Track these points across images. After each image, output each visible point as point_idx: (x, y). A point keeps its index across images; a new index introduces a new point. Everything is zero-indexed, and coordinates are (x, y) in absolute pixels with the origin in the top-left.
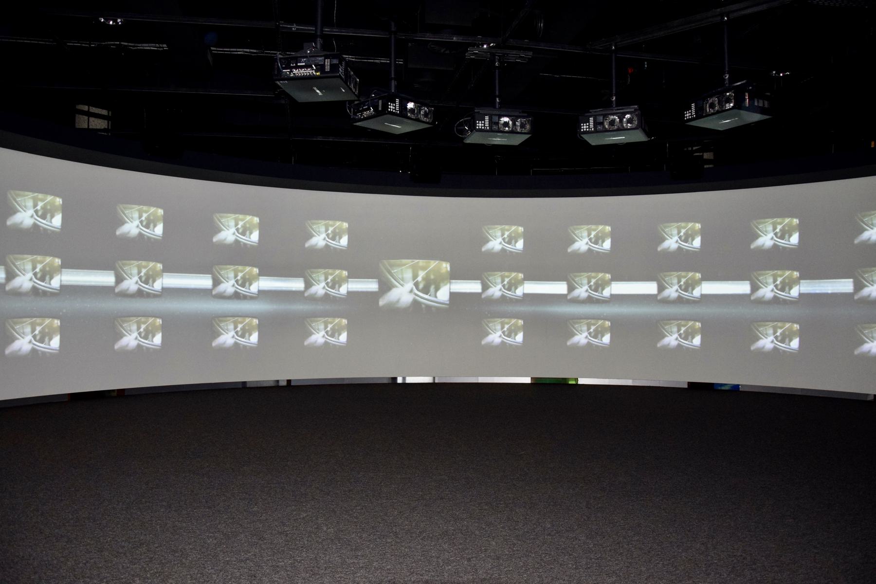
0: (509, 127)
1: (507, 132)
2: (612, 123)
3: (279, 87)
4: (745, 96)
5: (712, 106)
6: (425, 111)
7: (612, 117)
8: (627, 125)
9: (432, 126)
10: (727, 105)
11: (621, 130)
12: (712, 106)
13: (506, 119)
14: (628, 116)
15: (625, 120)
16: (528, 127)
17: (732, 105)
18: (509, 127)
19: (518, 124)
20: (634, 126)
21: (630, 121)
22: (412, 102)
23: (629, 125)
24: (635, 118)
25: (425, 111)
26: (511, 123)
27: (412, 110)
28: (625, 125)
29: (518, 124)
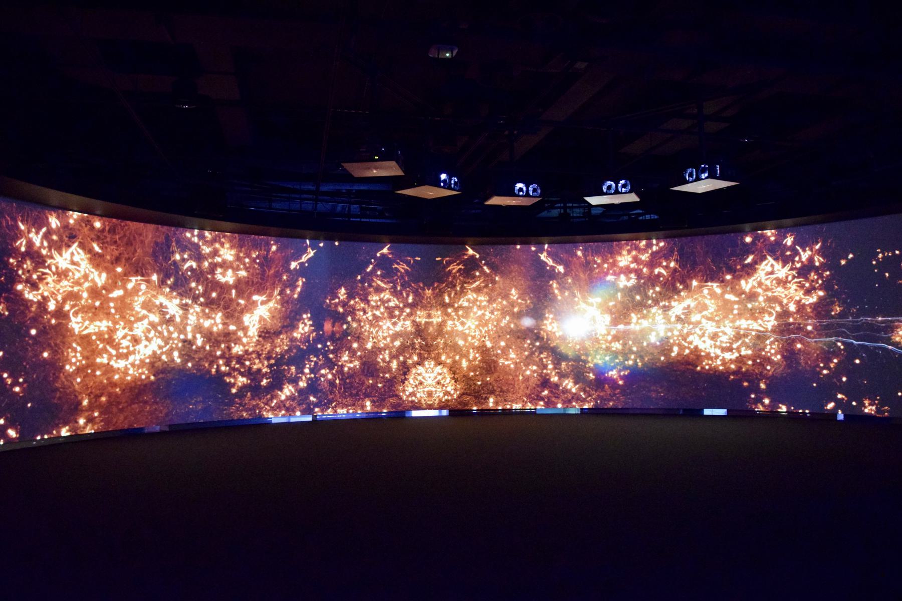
1: (521, 196)
4: (716, 167)
5: (691, 175)
6: (455, 182)
7: (609, 183)
9: (458, 193)
10: (703, 175)
11: (617, 192)
12: (691, 175)
13: (519, 185)
14: (622, 182)
15: (620, 185)
16: (539, 191)
17: (706, 175)
18: (523, 192)
19: (531, 189)
20: (628, 190)
21: (624, 186)
23: (623, 189)
24: (628, 182)
25: (455, 182)
26: (524, 189)
27: (444, 181)
28: (620, 190)
29: (531, 189)
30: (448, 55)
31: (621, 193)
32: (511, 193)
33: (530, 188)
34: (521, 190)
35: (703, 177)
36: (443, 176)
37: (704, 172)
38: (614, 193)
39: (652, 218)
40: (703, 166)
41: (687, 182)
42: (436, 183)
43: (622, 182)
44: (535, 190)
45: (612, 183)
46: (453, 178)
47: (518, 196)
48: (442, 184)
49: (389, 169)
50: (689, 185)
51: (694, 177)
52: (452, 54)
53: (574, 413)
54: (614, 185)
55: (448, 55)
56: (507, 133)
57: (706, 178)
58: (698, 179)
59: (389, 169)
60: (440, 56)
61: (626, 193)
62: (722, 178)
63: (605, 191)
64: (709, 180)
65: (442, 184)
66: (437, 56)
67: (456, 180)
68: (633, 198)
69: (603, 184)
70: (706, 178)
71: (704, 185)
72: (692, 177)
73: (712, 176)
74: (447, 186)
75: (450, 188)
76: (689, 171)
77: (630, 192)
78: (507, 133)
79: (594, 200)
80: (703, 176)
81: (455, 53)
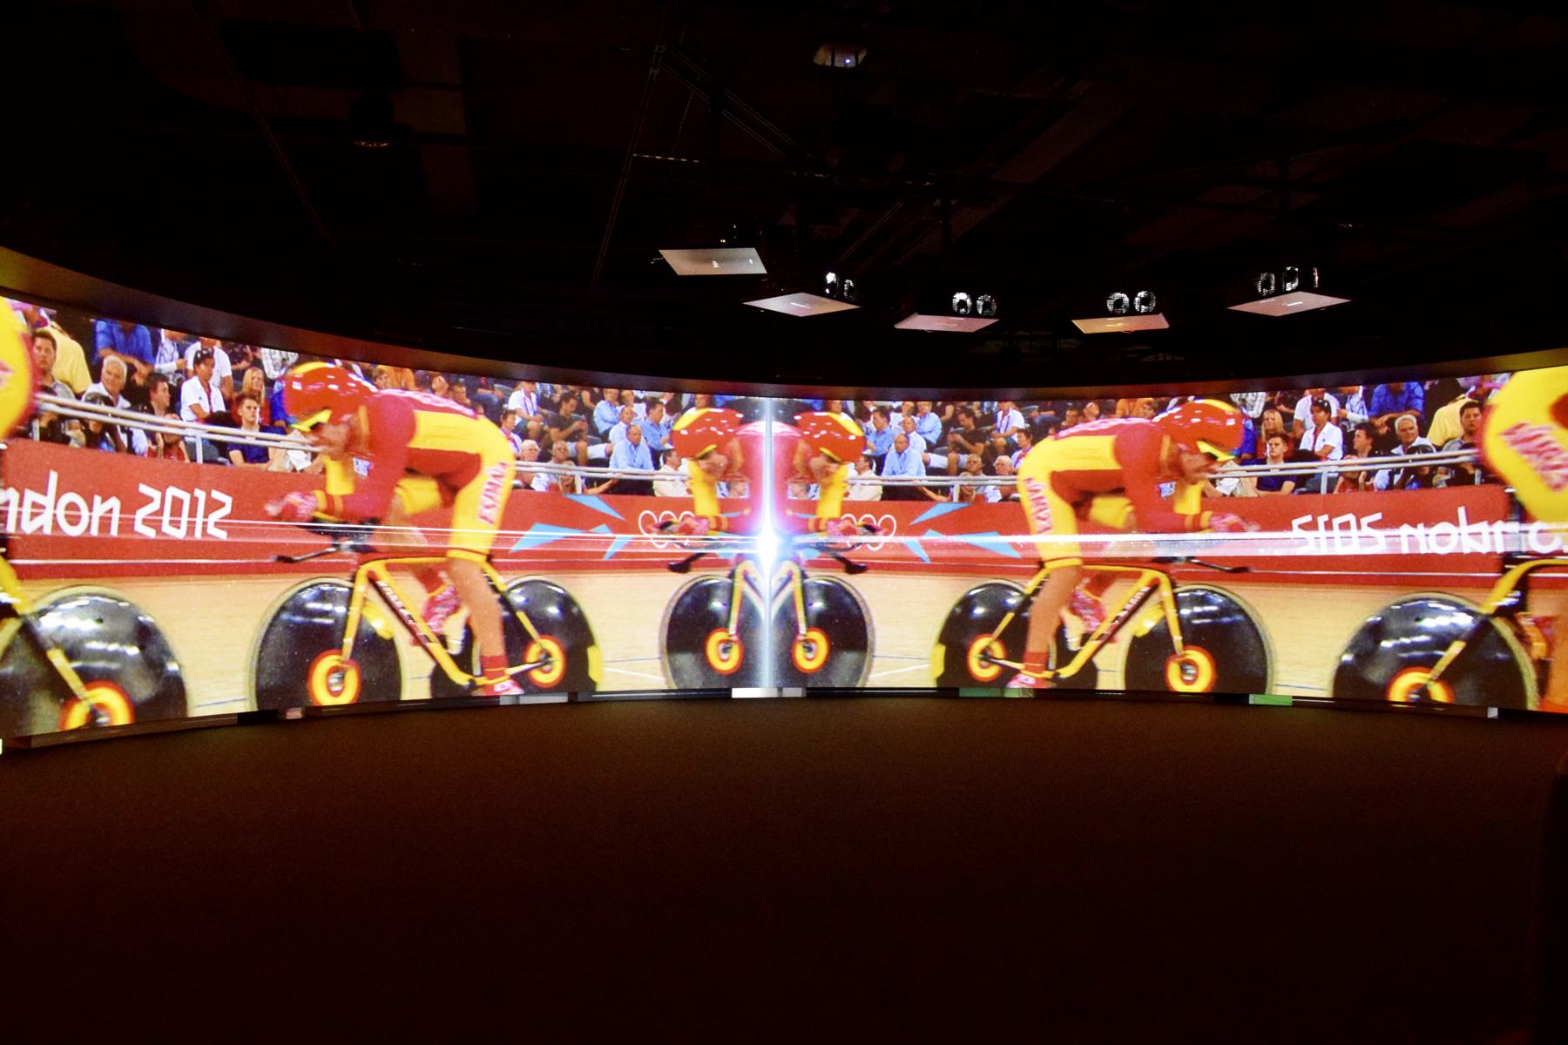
0: (966, 308)
2: (1119, 303)
3: (661, 256)
5: (1266, 284)
7: (1118, 295)
8: (1140, 308)
9: (853, 307)
10: (1288, 284)
11: (1132, 312)
13: (960, 296)
14: (1142, 294)
15: (1137, 299)
16: (994, 307)
17: (1295, 285)
18: (966, 310)
19: (980, 303)
20: (1152, 309)
21: (1144, 301)
22: (832, 272)
23: (1143, 307)
26: (969, 302)
28: (1137, 307)
29: (980, 303)
30: (848, 61)
31: (1139, 314)
32: (946, 310)
33: (978, 302)
34: (962, 303)
35: (1289, 289)
36: (831, 277)
37: (1292, 281)
38: (1126, 315)
39: (1161, 359)
40: (1289, 268)
41: (1260, 297)
42: (816, 287)
43: (1142, 294)
44: (986, 305)
45: (1123, 295)
46: (847, 281)
47: (958, 314)
48: (827, 291)
49: (750, 263)
50: (1262, 302)
51: (1273, 288)
52: (857, 59)
53: (1017, 696)
54: (1126, 299)
55: (848, 61)
56: (938, 202)
57: (1292, 291)
58: (1280, 291)
59: (750, 263)
60: (838, 64)
61: (1147, 313)
62: (1321, 291)
63: (1110, 308)
64: (1301, 294)
65: (827, 291)
66: (829, 63)
67: (852, 284)
68: (1160, 322)
69: (1107, 297)
70: (1292, 291)
71: (1298, 301)
72: (1269, 288)
73: (1306, 286)
74: (836, 293)
75: (841, 299)
76: (1263, 277)
77: (1155, 312)
78: (938, 202)
79: (1087, 326)
80: (1289, 287)
81: (861, 57)
